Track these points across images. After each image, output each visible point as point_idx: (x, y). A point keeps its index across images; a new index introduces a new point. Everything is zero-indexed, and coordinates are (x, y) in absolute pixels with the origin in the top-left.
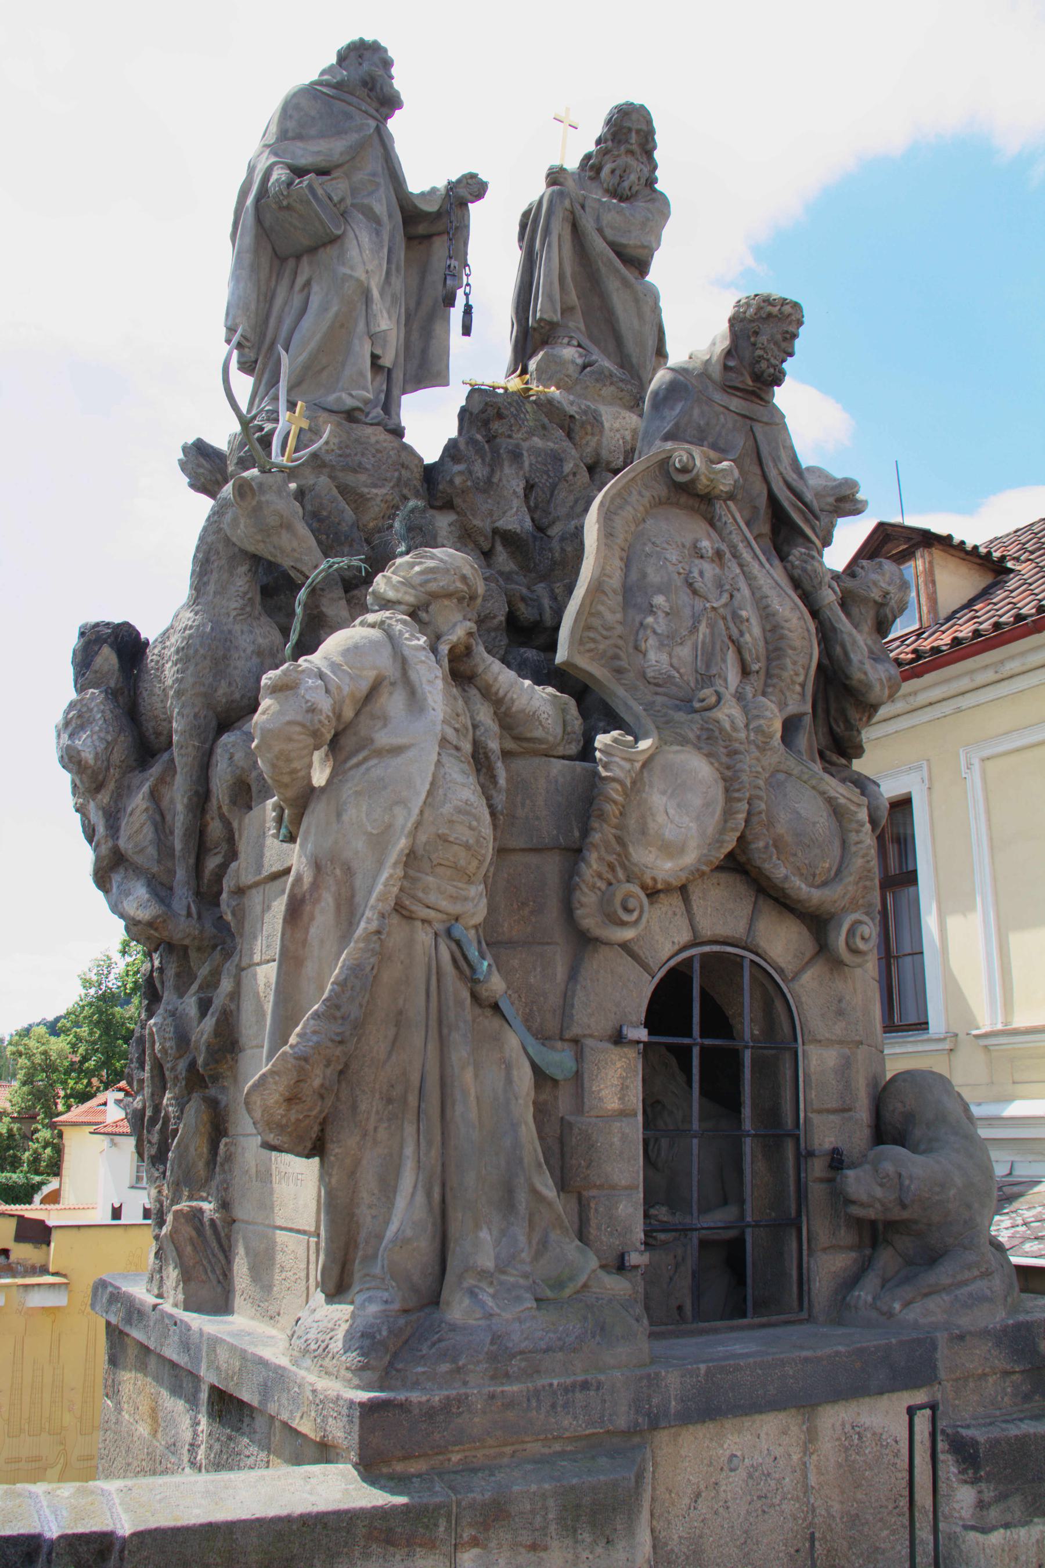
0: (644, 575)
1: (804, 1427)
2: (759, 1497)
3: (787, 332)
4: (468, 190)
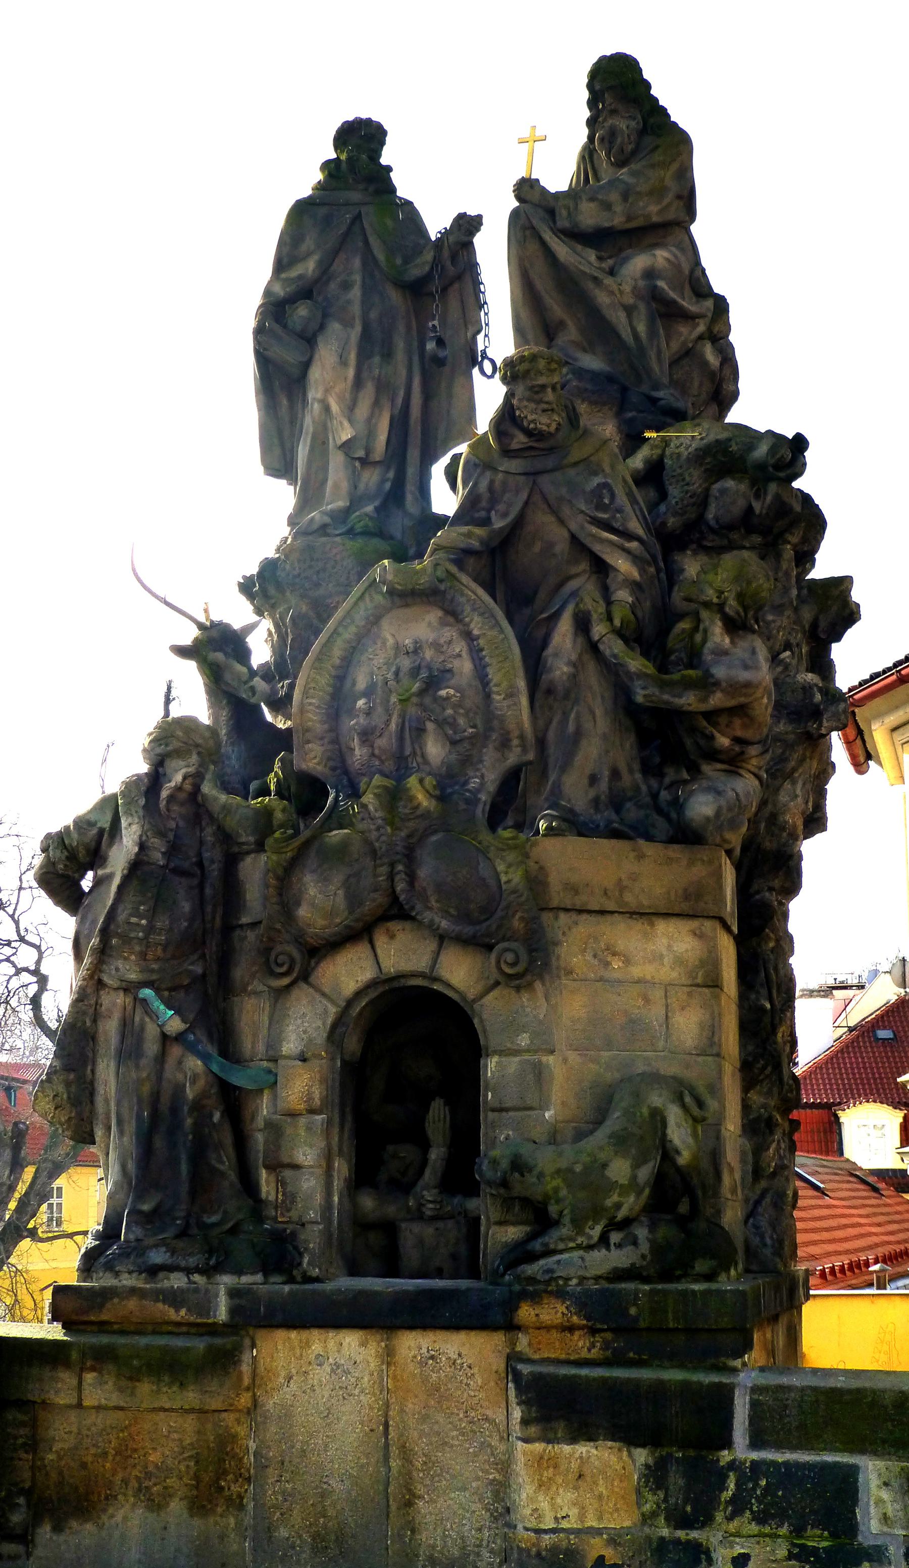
0: (354, 684)
1: (383, 1344)
2: (341, 1388)
3: (533, 387)
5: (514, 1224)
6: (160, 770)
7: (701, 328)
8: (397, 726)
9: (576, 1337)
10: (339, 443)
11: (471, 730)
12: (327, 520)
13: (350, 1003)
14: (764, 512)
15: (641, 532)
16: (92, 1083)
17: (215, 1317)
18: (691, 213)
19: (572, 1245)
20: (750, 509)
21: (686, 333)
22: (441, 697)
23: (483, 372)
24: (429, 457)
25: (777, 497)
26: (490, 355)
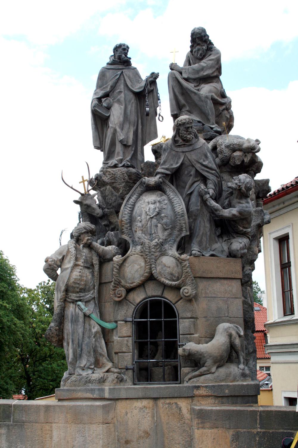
0: (136, 213)
4: (153, 79)
5: (189, 367)
6: (80, 238)
7: (224, 107)
8: (150, 225)
9: (210, 399)
10: (119, 140)
11: (171, 226)
12: (117, 162)
13: (138, 305)
14: (248, 162)
15: (216, 168)
16: (63, 330)
17: (104, 396)
18: (220, 73)
19: (208, 372)
20: (243, 161)
21: (221, 108)
22: (162, 216)
23: (159, 120)
24: (144, 143)
25: (252, 157)
26: (161, 115)
